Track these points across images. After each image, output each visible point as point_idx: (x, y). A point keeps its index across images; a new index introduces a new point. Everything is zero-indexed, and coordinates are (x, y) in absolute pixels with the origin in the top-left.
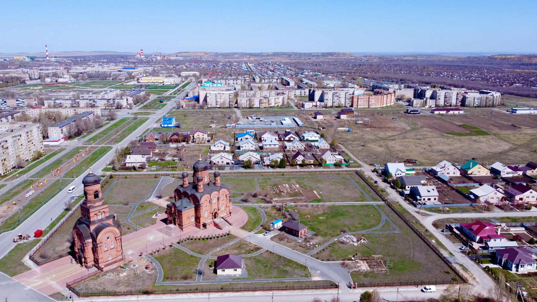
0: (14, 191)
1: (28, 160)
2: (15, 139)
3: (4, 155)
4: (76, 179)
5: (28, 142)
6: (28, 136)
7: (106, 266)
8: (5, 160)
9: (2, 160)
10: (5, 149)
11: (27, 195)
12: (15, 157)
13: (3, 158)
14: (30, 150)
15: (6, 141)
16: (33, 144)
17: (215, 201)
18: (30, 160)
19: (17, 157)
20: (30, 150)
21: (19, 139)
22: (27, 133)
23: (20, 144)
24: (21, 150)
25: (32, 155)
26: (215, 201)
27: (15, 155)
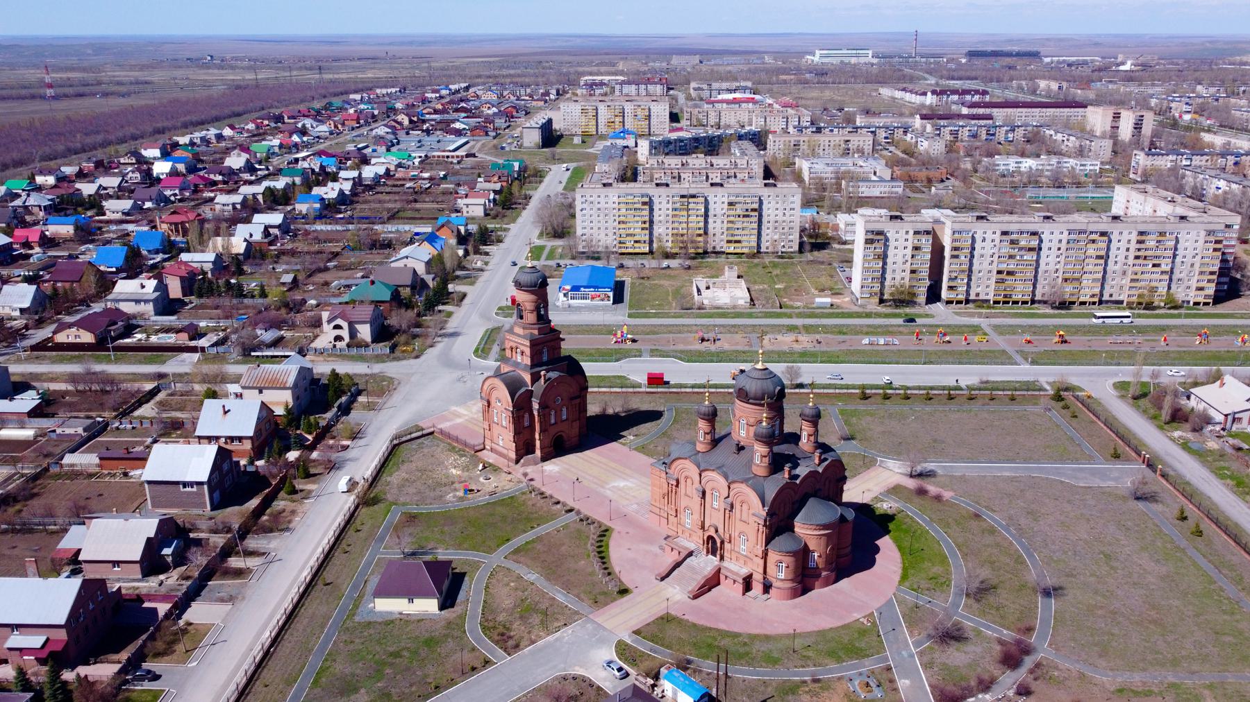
0: (891, 329)
1: (1122, 302)
2: (1072, 236)
3: (1012, 261)
4: (1028, 366)
5: (1137, 257)
6: (1139, 242)
7: (492, 450)
8: (1010, 273)
9: (999, 272)
10: (1021, 249)
11: (866, 341)
12: (1060, 280)
13: (1003, 267)
14: (1132, 280)
15: (1034, 234)
16: (1156, 269)
17: (716, 504)
18: (1125, 304)
19: (1066, 280)
20: (1132, 280)
21: (1094, 241)
22: (1141, 233)
23: (1091, 252)
24: (1090, 268)
25: (1139, 296)
26: (716, 504)
27: (1060, 274)
